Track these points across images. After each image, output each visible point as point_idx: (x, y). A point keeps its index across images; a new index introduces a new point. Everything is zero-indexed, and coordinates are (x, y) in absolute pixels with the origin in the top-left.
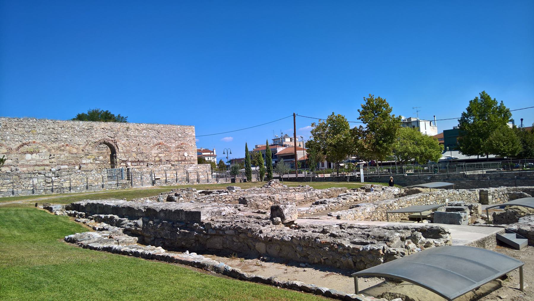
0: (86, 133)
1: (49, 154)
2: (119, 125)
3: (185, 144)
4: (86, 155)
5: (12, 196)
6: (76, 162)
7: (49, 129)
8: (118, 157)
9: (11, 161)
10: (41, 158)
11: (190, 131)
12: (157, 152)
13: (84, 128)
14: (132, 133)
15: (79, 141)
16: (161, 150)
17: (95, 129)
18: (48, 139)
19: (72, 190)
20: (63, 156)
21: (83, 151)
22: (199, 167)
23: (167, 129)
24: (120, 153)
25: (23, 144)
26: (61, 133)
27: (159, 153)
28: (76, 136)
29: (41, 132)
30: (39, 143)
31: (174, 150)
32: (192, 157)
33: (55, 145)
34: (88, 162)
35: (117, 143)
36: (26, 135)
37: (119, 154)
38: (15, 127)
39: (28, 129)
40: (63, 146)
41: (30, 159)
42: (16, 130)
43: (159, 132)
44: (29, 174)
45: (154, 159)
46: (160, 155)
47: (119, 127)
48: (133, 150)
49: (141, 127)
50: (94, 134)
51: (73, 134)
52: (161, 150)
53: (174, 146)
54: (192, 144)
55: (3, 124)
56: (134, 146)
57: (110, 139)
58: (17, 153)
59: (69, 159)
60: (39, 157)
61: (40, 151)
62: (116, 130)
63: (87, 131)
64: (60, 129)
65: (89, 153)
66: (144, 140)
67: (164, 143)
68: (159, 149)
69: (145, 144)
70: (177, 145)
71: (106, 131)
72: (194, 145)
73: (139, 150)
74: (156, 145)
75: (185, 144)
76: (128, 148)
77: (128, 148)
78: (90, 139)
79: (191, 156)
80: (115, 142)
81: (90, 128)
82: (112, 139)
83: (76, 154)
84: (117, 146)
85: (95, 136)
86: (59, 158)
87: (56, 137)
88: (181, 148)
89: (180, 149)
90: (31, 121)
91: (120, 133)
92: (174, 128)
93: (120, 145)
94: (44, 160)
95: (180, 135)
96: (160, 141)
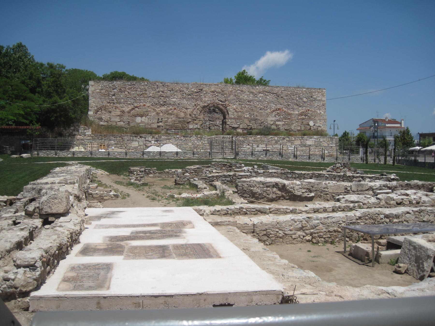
0: (195, 96)
1: (157, 117)
2: (231, 87)
3: (311, 111)
4: (193, 120)
5: (90, 156)
6: (183, 127)
7: (158, 92)
8: (228, 123)
9: (123, 123)
10: (150, 122)
11: (319, 95)
12: (274, 119)
13: (193, 91)
15: (188, 105)
16: (279, 117)
17: (205, 92)
18: (157, 102)
19: (145, 155)
20: (170, 120)
21: (190, 115)
22: (321, 140)
23: (289, 93)
24: (231, 119)
25: (135, 107)
26: (170, 96)
27: (277, 121)
28: (185, 100)
29: (151, 95)
30: (148, 107)
31: (296, 118)
32: (320, 126)
33: (163, 108)
34: (195, 127)
35: (228, 107)
36: (138, 99)
37: (230, 120)
38: (128, 91)
39: (139, 92)
40: (171, 109)
41: (140, 121)
42: (129, 93)
43: (278, 96)
44: (132, 137)
46: (278, 123)
47: (230, 90)
48: (246, 116)
49: (257, 89)
50: (203, 98)
52: (279, 117)
53: (297, 113)
55: (118, 88)
56: (247, 111)
57: (221, 103)
58: (129, 116)
59: (176, 124)
60: (148, 121)
61: (149, 114)
62: (227, 93)
63: (195, 94)
64: (169, 92)
65: (197, 118)
66: (260, 105)
67: (284, 109)
69: (261, 109)
70: (301, 111)
71: (217, 94)
72: (323, 113)
73: (252, 116)
74: (274, 111)
75: (311, 111)
76: (240, 114)
77: (240, 114)
78: (199, 102)
79: (318, 125)
80: (225, 107)
81: (199, 90)
83: (183, 118)
84: (227, 111)
85: (204, 99)
86: (166, 122)
87: (165, 100)
88: (305, 115)
89: (304, 117)
90: (143, 84)
91: (232, 97)
92: (298, 92)
94: (152, 123)
95: (305, 100)
96: (279, 106)
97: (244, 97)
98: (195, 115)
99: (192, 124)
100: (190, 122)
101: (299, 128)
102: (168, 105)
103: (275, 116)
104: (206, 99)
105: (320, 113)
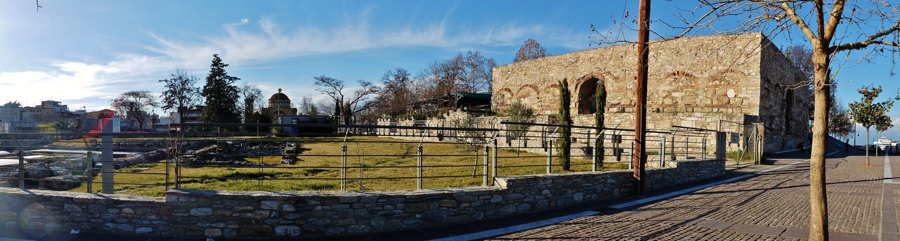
12: (668, 88)
14: (631, 58)
31: (704, 85)
45: (661, 102)
46: (675, 94)
52: (678, 85)
54: (751, 71)
68: (674, 84)
72: (754, 74)
93: (610, 79)
97: (628, 59)
101: (709, 102)
103: (670, 84)
105: (749, 74)
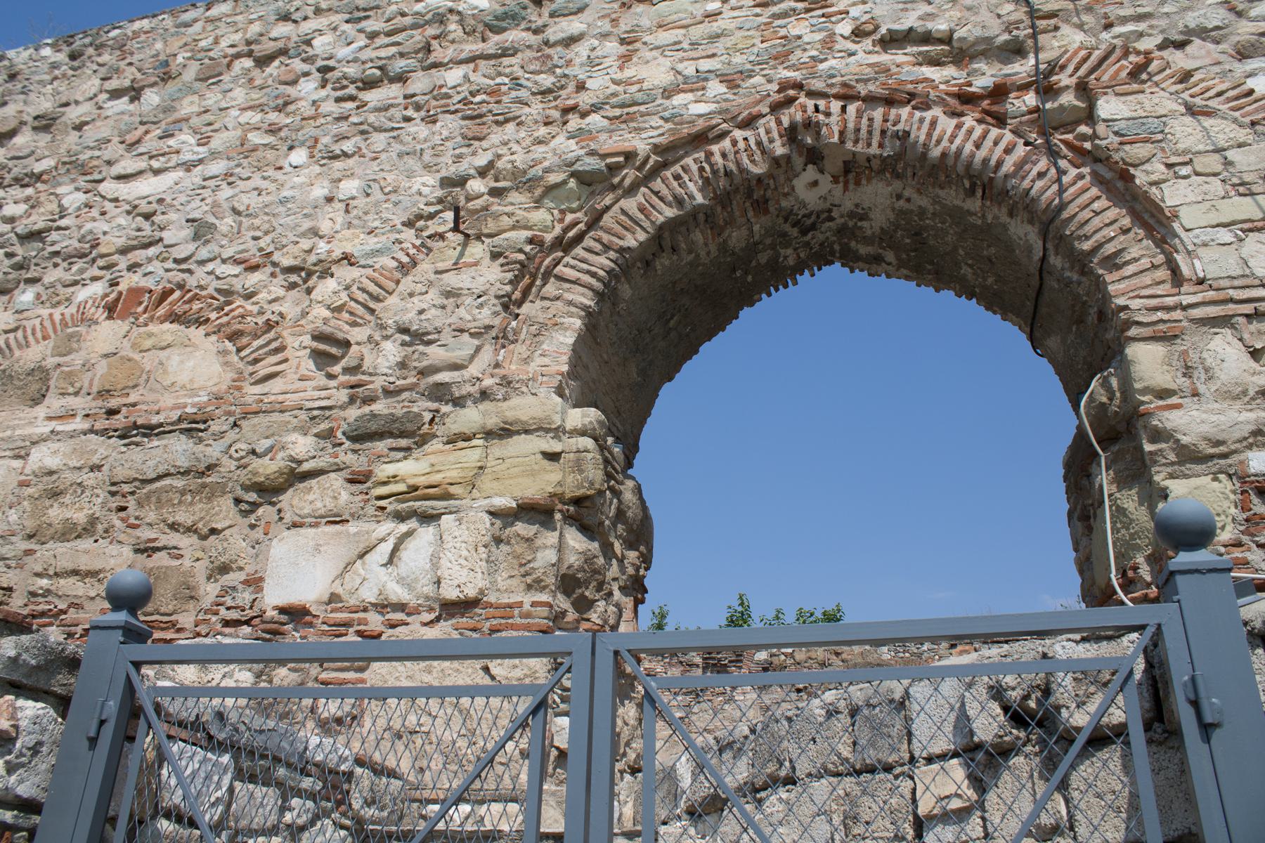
28: (299, 156)
35: (1107, 107)
51: (256, 138)
57: (944, 76)
59: (70, 532)
65: (440, 393)
82: (985, 76)
83: (193, 426)
93: (1186, 133)
98: (415, 336)
99: (337, 520)
100: (297, 476)
102: (51, 276)
104: (655, 72)
